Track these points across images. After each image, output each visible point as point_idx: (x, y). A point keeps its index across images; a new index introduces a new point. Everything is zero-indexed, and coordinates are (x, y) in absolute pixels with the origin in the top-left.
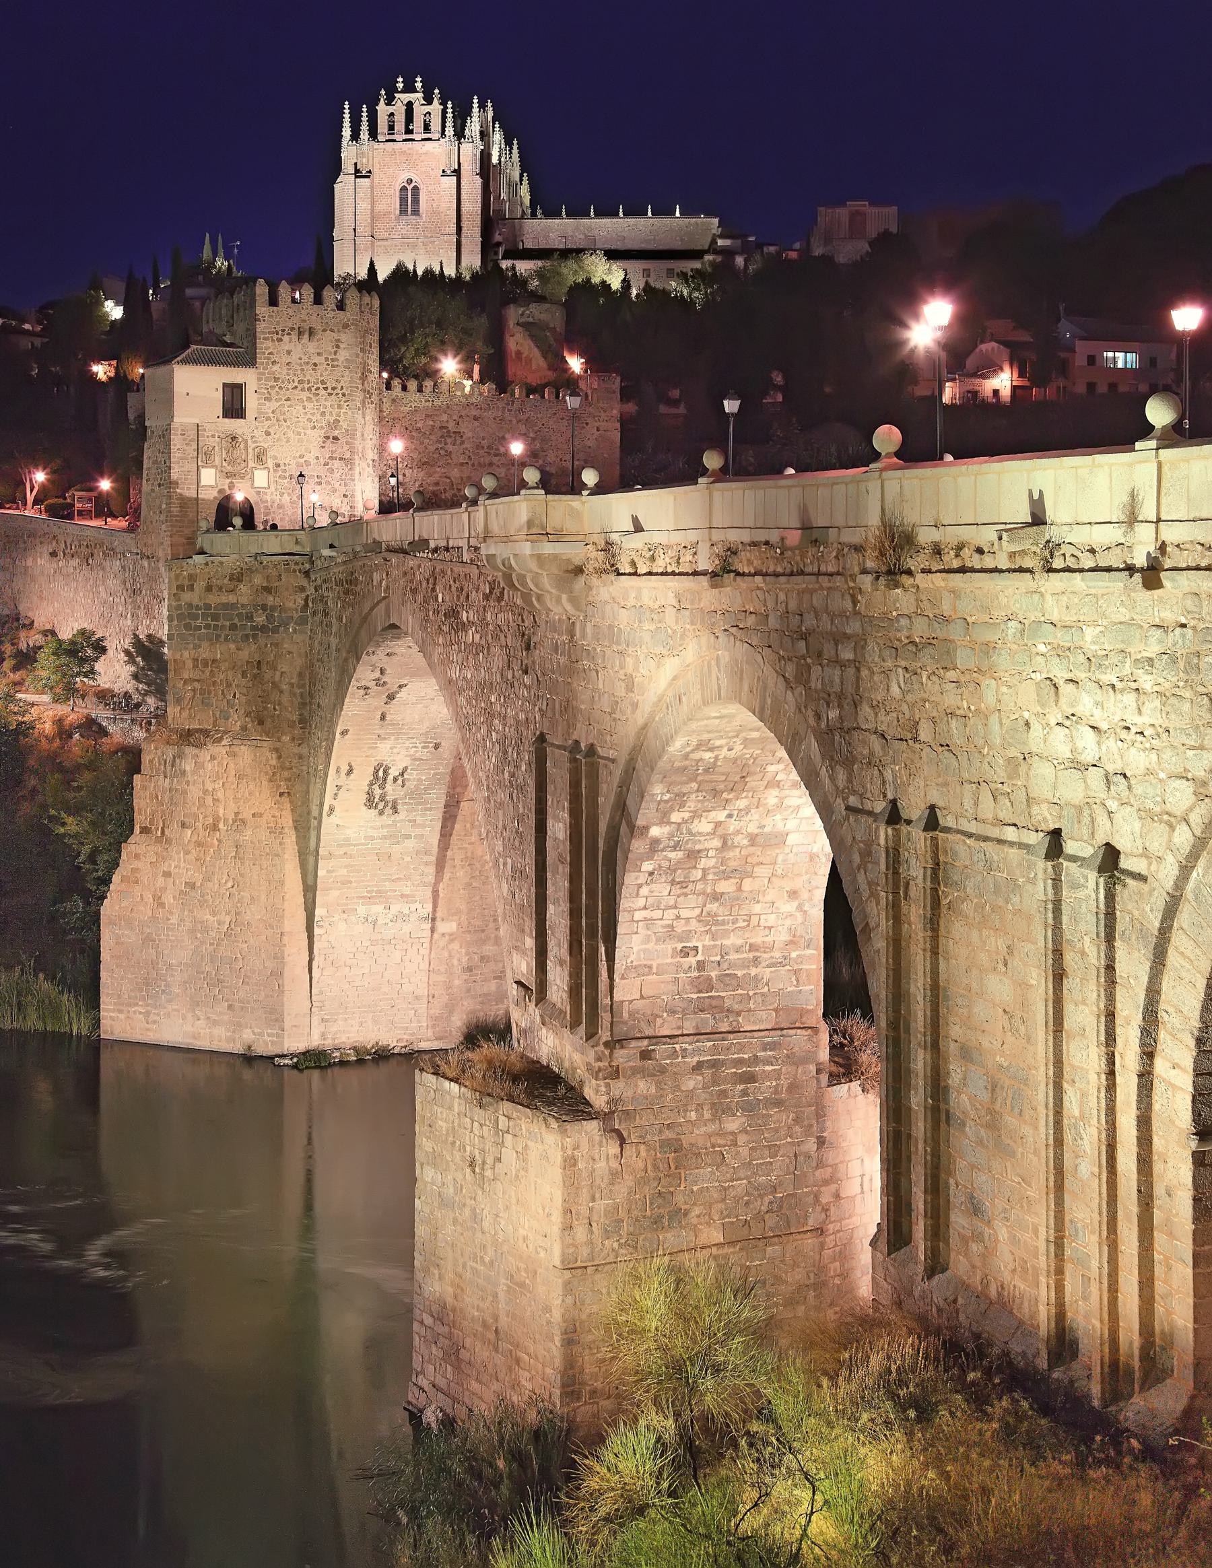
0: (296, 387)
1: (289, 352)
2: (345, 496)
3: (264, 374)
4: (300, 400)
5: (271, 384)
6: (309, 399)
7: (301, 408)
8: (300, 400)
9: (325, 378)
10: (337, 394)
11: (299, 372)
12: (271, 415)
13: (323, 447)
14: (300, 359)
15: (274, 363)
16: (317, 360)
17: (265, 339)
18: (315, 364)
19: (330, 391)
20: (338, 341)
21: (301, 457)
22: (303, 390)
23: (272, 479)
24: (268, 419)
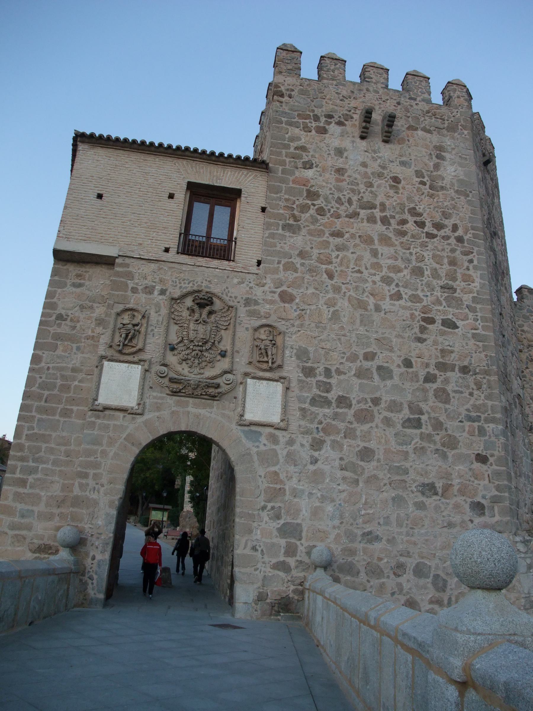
0: (355, 215)
1: (340, 152)
2: (482, 459)
3: (283, 181)
4: (368, 240)
5: (301, 201)
6: (385, 240)
7: (367, 255)
8: (368, 240)
9: (420, 209)
10: (446, 238)
11: (362, 187)
12: (297, 261)
13: (420, 340)
14: (364, 165)
15: (308, 166)
16: (396, 170)
17: (290, 124)
18: (396, 180)
19: (429, 228)
20: (440, 148)
21: (369, 356)
22: (371, 220)
23: (294, 405)
24: (290, 267)
